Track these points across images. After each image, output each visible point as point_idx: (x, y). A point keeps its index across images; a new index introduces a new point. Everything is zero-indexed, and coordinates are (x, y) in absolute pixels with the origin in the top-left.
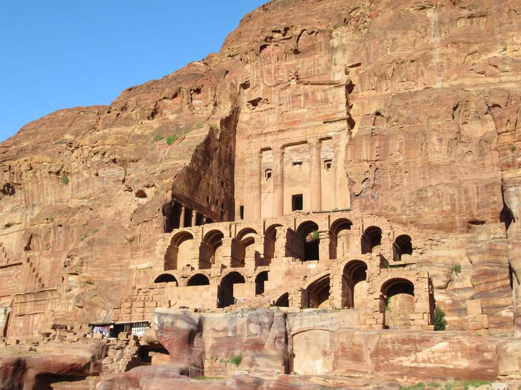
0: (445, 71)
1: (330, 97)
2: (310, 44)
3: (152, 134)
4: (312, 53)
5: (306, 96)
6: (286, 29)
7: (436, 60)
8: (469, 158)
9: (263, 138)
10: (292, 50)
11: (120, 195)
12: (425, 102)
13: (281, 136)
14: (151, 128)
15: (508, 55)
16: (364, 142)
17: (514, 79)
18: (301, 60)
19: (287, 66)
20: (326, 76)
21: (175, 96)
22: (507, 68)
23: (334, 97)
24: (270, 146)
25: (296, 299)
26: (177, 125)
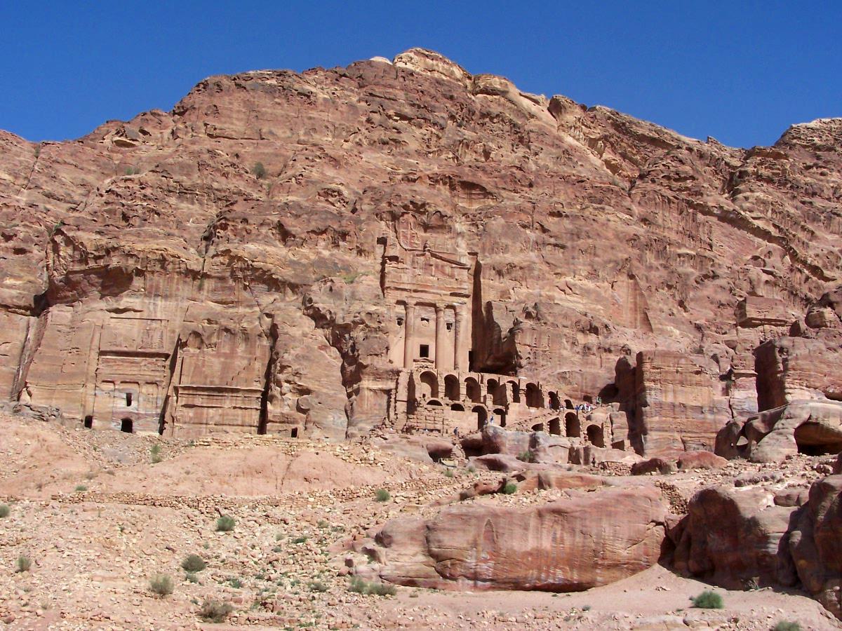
0: (540, 282)
1: (456, 273)
2: (441, 223)
3: (312, 265)
4: (440, 230)
5: (437, 267)
6: (423, 205)
7: (536, 273)
8: (578, 356)
9: (399, 292)
10: (424, 223)
11: (301, 317)
12: (560, 315)
13: (414, 295)
14: (308, 258)
15: (577, 282)
16: (528, 334)
17: (580, 300)
18: (434, 235)
19: (422, 236)
20: (454, 256)
21: (324, 232)
22: (577, 292)
23: (458, 275)
24: (405, 300)
25: (546, 428)
26: (336, 264)
